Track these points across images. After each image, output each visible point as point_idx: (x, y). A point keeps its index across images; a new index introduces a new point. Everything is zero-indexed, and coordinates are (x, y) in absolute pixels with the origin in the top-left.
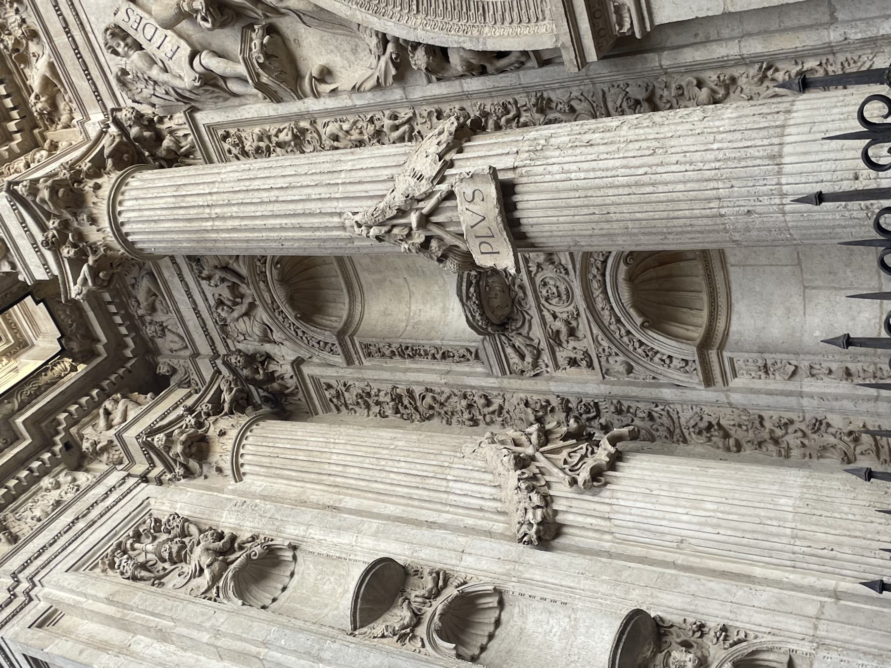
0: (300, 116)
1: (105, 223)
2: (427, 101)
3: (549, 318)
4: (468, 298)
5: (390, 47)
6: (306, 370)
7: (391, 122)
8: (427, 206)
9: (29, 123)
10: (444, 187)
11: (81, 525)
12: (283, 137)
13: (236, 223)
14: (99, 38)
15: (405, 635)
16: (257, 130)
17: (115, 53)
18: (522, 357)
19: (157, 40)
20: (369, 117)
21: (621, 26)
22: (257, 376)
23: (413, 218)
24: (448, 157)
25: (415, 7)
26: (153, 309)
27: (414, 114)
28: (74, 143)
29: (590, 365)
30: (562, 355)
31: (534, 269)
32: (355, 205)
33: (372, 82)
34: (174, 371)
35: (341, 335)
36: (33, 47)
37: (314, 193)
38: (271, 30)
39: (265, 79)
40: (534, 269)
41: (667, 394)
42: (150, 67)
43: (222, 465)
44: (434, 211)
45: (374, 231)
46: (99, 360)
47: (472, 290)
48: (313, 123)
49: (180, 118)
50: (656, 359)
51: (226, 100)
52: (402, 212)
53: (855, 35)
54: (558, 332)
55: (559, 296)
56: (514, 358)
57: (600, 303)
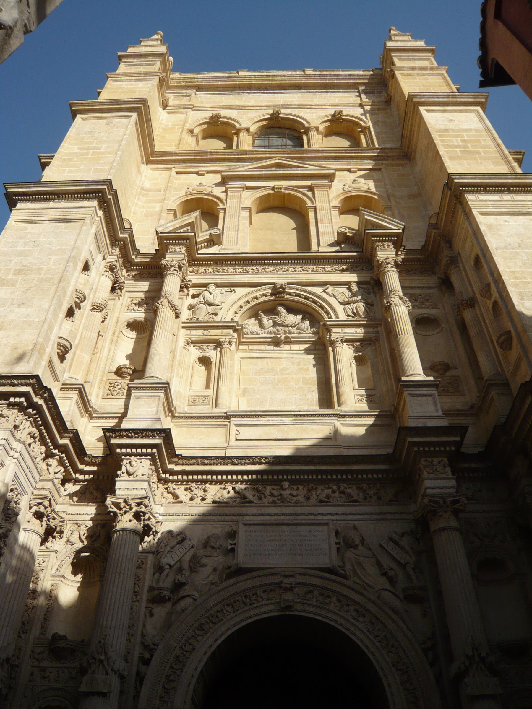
4: (67, 644)
7: (131, 634)
8: (105, 663)
9: (166, 481)
10: (109, 671)
11: (27, 471)
12: (137, 587)
13: (116, 583)
16: (141, 577)
17: (178, 535)
18: (39, 654)
19: (178, 552)
20: (135, 625)
22: (56, 532)
23: (103, 658)
24: (117, 673)
27: (131, 643)
28: (155, 497)
29: (30, 681)
35: (63, 576)
36: (189, 496)
38: (169, 599)
39: (156, 592)
42: (170, 547)
44: (104, 666)
45: (102, 641)
47: (69, 646)
51: (154, 568)
52: (106, 653)
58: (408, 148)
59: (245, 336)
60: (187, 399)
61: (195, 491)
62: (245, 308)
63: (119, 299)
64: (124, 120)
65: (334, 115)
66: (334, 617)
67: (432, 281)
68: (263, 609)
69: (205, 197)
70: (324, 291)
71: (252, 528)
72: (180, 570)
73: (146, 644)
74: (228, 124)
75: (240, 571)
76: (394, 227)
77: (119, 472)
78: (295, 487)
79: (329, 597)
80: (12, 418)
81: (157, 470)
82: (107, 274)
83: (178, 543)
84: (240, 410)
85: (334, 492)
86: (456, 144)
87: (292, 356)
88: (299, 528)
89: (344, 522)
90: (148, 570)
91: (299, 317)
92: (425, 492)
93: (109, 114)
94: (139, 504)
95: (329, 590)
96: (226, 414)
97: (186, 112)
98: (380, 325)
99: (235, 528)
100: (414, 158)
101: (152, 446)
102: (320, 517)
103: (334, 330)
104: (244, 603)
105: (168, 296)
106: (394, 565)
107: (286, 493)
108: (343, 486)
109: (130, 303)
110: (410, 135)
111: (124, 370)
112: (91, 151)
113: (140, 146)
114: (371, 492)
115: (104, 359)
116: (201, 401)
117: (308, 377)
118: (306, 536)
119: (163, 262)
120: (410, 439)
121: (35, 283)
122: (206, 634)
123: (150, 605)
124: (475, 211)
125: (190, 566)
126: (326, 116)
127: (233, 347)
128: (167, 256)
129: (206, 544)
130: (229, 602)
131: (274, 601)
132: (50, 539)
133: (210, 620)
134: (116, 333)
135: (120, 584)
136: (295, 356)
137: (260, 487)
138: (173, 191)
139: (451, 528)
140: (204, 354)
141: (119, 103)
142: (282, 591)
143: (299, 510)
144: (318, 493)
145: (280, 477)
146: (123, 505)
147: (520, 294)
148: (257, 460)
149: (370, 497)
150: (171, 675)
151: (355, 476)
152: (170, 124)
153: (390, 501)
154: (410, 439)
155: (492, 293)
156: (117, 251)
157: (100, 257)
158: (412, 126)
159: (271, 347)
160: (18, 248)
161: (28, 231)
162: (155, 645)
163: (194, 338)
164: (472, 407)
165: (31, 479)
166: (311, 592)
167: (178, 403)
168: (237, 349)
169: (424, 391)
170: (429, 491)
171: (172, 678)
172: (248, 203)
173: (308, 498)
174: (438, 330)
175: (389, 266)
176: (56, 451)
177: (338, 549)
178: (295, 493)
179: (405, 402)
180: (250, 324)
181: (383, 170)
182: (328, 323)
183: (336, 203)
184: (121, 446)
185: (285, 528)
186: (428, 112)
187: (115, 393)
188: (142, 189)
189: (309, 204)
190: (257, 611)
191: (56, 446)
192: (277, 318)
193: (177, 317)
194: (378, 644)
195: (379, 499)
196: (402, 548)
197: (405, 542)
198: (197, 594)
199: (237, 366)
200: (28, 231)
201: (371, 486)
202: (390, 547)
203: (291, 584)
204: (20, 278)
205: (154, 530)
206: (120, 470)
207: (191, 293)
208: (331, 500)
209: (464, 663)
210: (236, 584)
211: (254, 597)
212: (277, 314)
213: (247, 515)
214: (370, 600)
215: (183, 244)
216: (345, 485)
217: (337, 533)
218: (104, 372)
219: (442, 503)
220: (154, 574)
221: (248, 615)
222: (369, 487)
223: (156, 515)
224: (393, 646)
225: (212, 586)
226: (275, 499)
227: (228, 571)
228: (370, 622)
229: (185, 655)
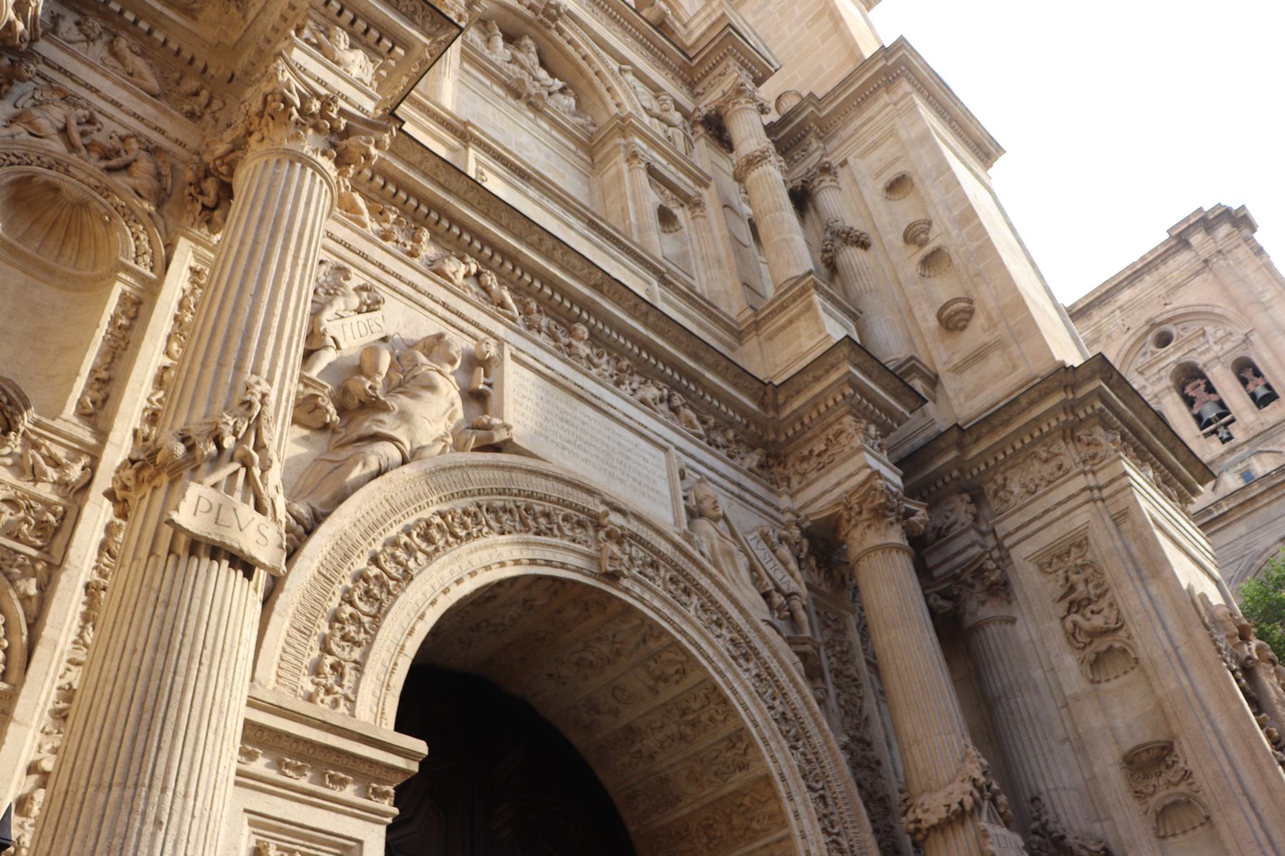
14: (383, 292)
25: (324, 572)
91: (558, 84)
96: (465, 127)
122: (437, 550)
148: (549, 243)
159: (501, 92)
166: (653, 565)
171: (351, 629)
192: (520, 56)
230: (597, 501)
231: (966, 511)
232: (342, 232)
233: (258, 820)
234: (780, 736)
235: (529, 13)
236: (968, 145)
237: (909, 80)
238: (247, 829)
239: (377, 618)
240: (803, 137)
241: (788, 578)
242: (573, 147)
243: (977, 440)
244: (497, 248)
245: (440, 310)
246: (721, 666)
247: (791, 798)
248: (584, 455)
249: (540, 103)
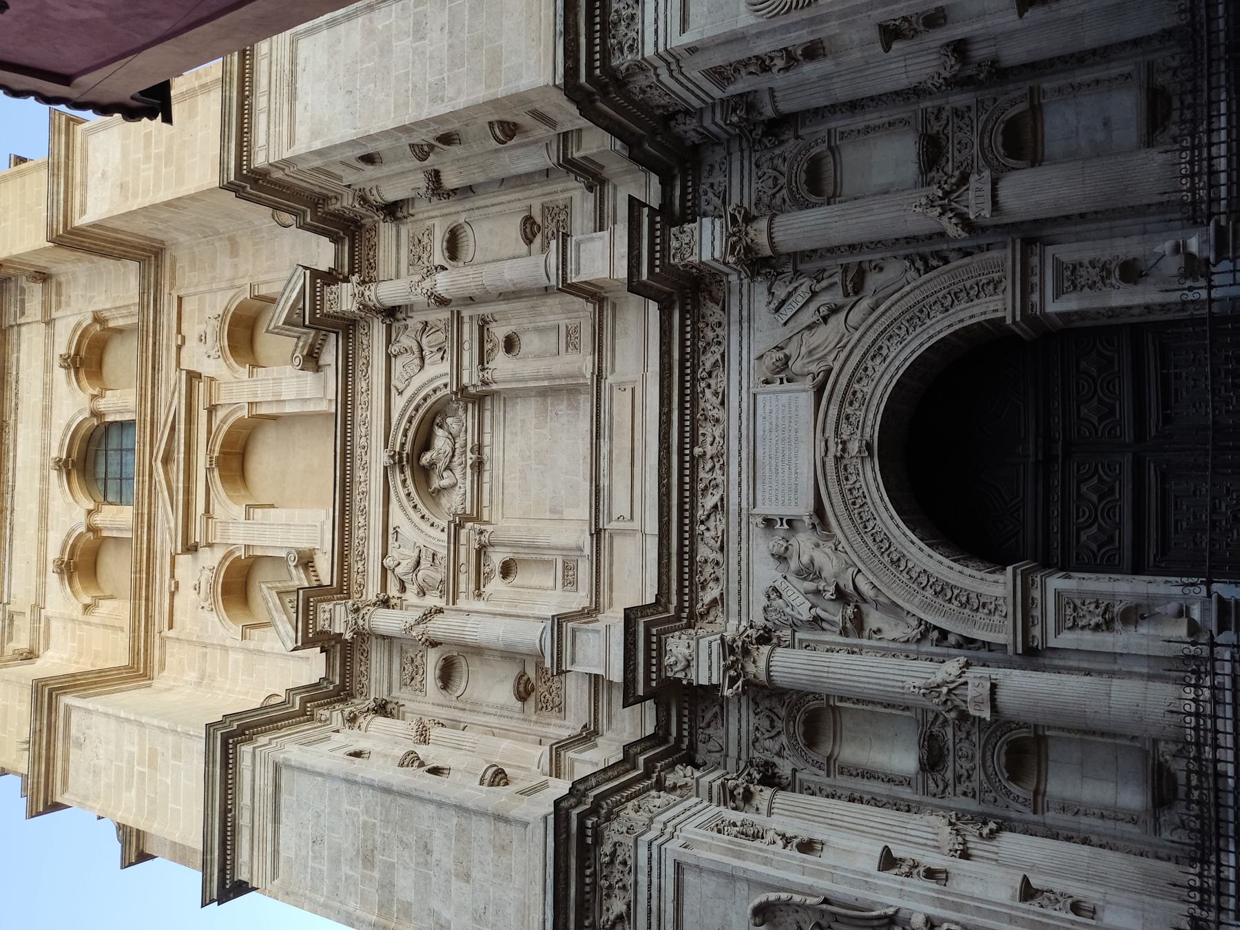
0: (856, 646)
1: (762, 664)
2: (927, 653)
3: (958, 767)
5: (922, 627)
6: (798, 775)
8: (952, 686)
9: (692, 616)
10: (961, 680)
11: (688, 813)
15: (909, 875)
17: (769, 597)
18: (937, 786)
19: (793, 597)
21: (1033, 642)
23: (945, 690)
26: (709, 725)
29: (974, 796)
30: (960, 789)
31: (957, 741)
32: (914, 680)
33: (906, 639)
34: (705, 764)
35: (829, 758)
36: (711, 584)
37: (891, 671)
38: (856, 607)
39: (849, 625)
40: (957, 741)
41: (1014, 815)
43: (760, 806)
44: (955, 688)
45: (922, 691)
46: (668, 746)
48: (861, 650)
49: (789, 632)
50: (1011, 797)
52: (938, 686)
53: (1124, 669)
54: (961, 776)
55: (967, 757)
56: (932, 785)
57: (989, 763)
58: (144, 250)
59: (468, 512)
60: (567, 593)
61: (706, 575)
62: (425, 511)
63: (403, 705)
64: (75, 718)
65: (67, 368)
66: (881, 388)
67: (386, 231)
68: (871, 481)
69: (221, 580)
70: (400, 393)
71: (759, 497)
72: (818, 592)
73: (919, 637)
74: (73, 547)
75: (819, 510)
76: (301, 282)
77: (685, 682)
78: (701, 438)
79: (854, 393)
80: (617, 838)
81: (679, 629)
82: (363, 726)
83: (780, 597)
84: (588, 518)
85: (709, 386)
86: (152, 172)
87: (501, 444)
88: (759, 433)
89: (752, 372)
90: (817, 638)
91: (439, 432)
92: (717, 261)
93: (60, 744)
94: (732, 651)
95: (845, 394)
97: (48, 620)
98: (458, 312)
99: (759, 520)
100: (162, 242)
101: (648, 635)
102: (744, 405)
103: (466, 380)
104: (861, 506)
105: (408, 625)
106: (813, 307)
107: (710, 451)
108: (701, 373)
109: (409, 688)
110: (122, 245)
111: (521, 689)
112: (137, 768)
113: (121, 691)
114: (710, 335)
115: (503, 721)
116: (571, 573)
117: (534, 421)
118: (771, 424)
119: (348, 636)
120: (645, 277)
121: (389, 832)
122: (904, 556)
123: (866, 633)
124: (286, 155)
125: (812, 581)
126: (69, 383)
127: (489, 528)
128: (337, 631)
129: (782, 558)
130: (861, 526)
131: (860, 466)
132: (777, 780)
133: (887, 550)
134: (460, 705)
135: (843, 671)
136: (501, 439)
137: (701, 486)
138: (207, 632)
139: (770, 228)
140: (498, 570)
141: (38, 729)
142: (846, 455)
143: (734, 433)
144: (710, 407)
145: (687, 458)
146: (732, 673)
147: (433, 101)
148: (664, 489)
149: (718, 336)
150: (960, 602)
151: (688, 356)
152: (70, 644)
153: (723, 309)
154: (645, 277)
155: (424, 143)
156: (324, 713)
157: (336, 736)
158: (106, 241)
160: (325, 868)
161: (292, 855)
162: (920, 624)
163: (472, 586)
164: (590, 188)
165: (700, 807)
166: (848, 417)
167: (574, 605)
168: (488, 523)
169: (572, 254)
170: (717, 255)
171: (964, 599)
172: (238, 511)
173: (717, 420)
174: (467, 228)
175: (367, 293)
176: (655, 775)
177: (789, 381)
178: (709, 440)
179: (586, 282)
180: (448, 505)
181: (181, 293)
182: (454, 390)
183: (243, 371)
184: (647, 680)
185: (759, 453)
186: (85, 213)
187: (557, 700)
188: (199, 684)
189: (244, 413)
190: (873, 489)
191: (647, 775)
192: (441, 465)
193: (440, 611)
194: (919, 330)
195: (720, 324)
196: (790, 295)
197: (781, 292)
198: (851, 570)
199: (516, 523)
200: (292, 855)
201: (701, 335)
202: (787, 311)
203: (837, 443)
204: (379, 857)
205: (762, 632)
206: (680, 680)
207: (397, 594)
208: (720, 390)
209: (950, 218)
210: (836, 516)
211: (855, 492)
212: (433, 465)
213: (740, 504)
214: (859, 340)
215: (315, 607)
216: (701, 370)
217: (767, 382)
218: (523, 719)
219: (734, 239)
220: (823, 629)
221: (878, 501)
222: (703, 337)
223: (742, 629)
224: (921, 311)
225: (840, 548)
226: (718, 466)
227: (818, 528)
228: (889, 340)
229: (934, 583)
230: (827, 459)
231: (685, 124)
232: (734, 607)
233: (1058, 632)
234: (924, 327)
235: (408, 472)
236: (252, 64)
237: (249, 161)
238: (1062, 636)
239: (952, 588)
240: (331, 214)
241: (799, 292)
242: (487, 414)
243: (633, 134)
244: (681, 518)
245: (744, 545)
246: (893, 369)
247: (962, 321)
248: (793, 459)
249: (476, 448)
